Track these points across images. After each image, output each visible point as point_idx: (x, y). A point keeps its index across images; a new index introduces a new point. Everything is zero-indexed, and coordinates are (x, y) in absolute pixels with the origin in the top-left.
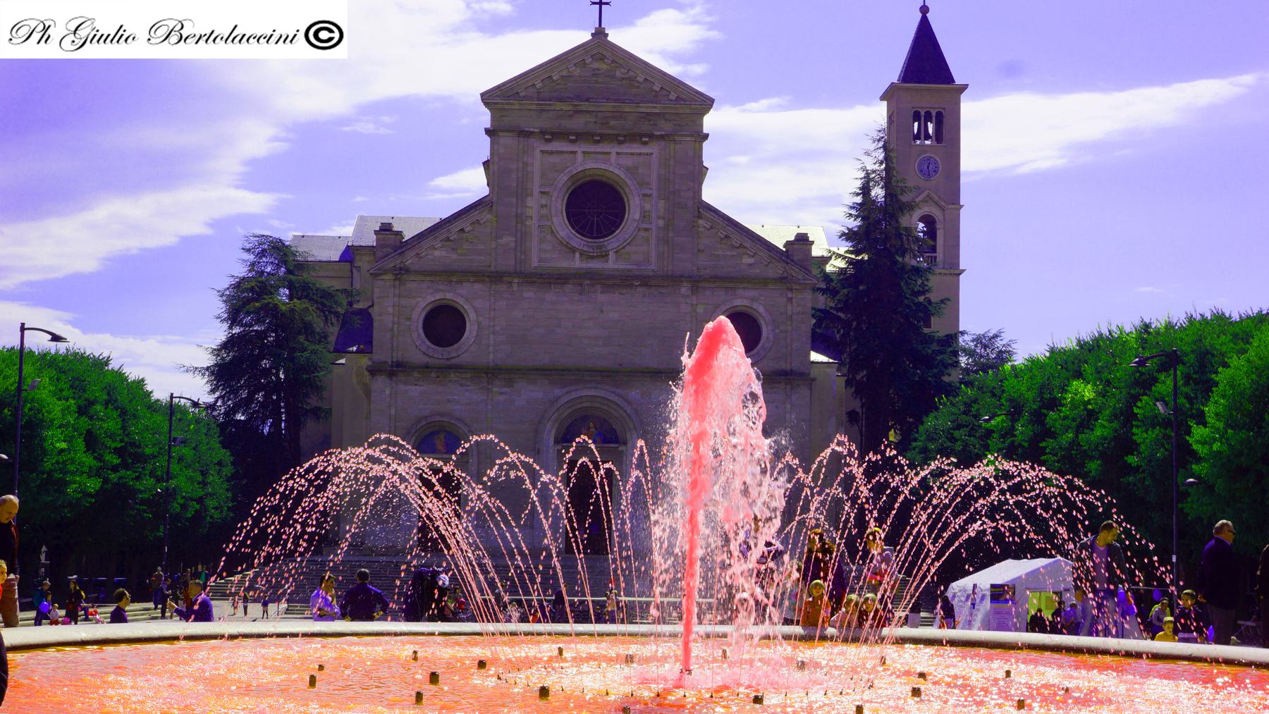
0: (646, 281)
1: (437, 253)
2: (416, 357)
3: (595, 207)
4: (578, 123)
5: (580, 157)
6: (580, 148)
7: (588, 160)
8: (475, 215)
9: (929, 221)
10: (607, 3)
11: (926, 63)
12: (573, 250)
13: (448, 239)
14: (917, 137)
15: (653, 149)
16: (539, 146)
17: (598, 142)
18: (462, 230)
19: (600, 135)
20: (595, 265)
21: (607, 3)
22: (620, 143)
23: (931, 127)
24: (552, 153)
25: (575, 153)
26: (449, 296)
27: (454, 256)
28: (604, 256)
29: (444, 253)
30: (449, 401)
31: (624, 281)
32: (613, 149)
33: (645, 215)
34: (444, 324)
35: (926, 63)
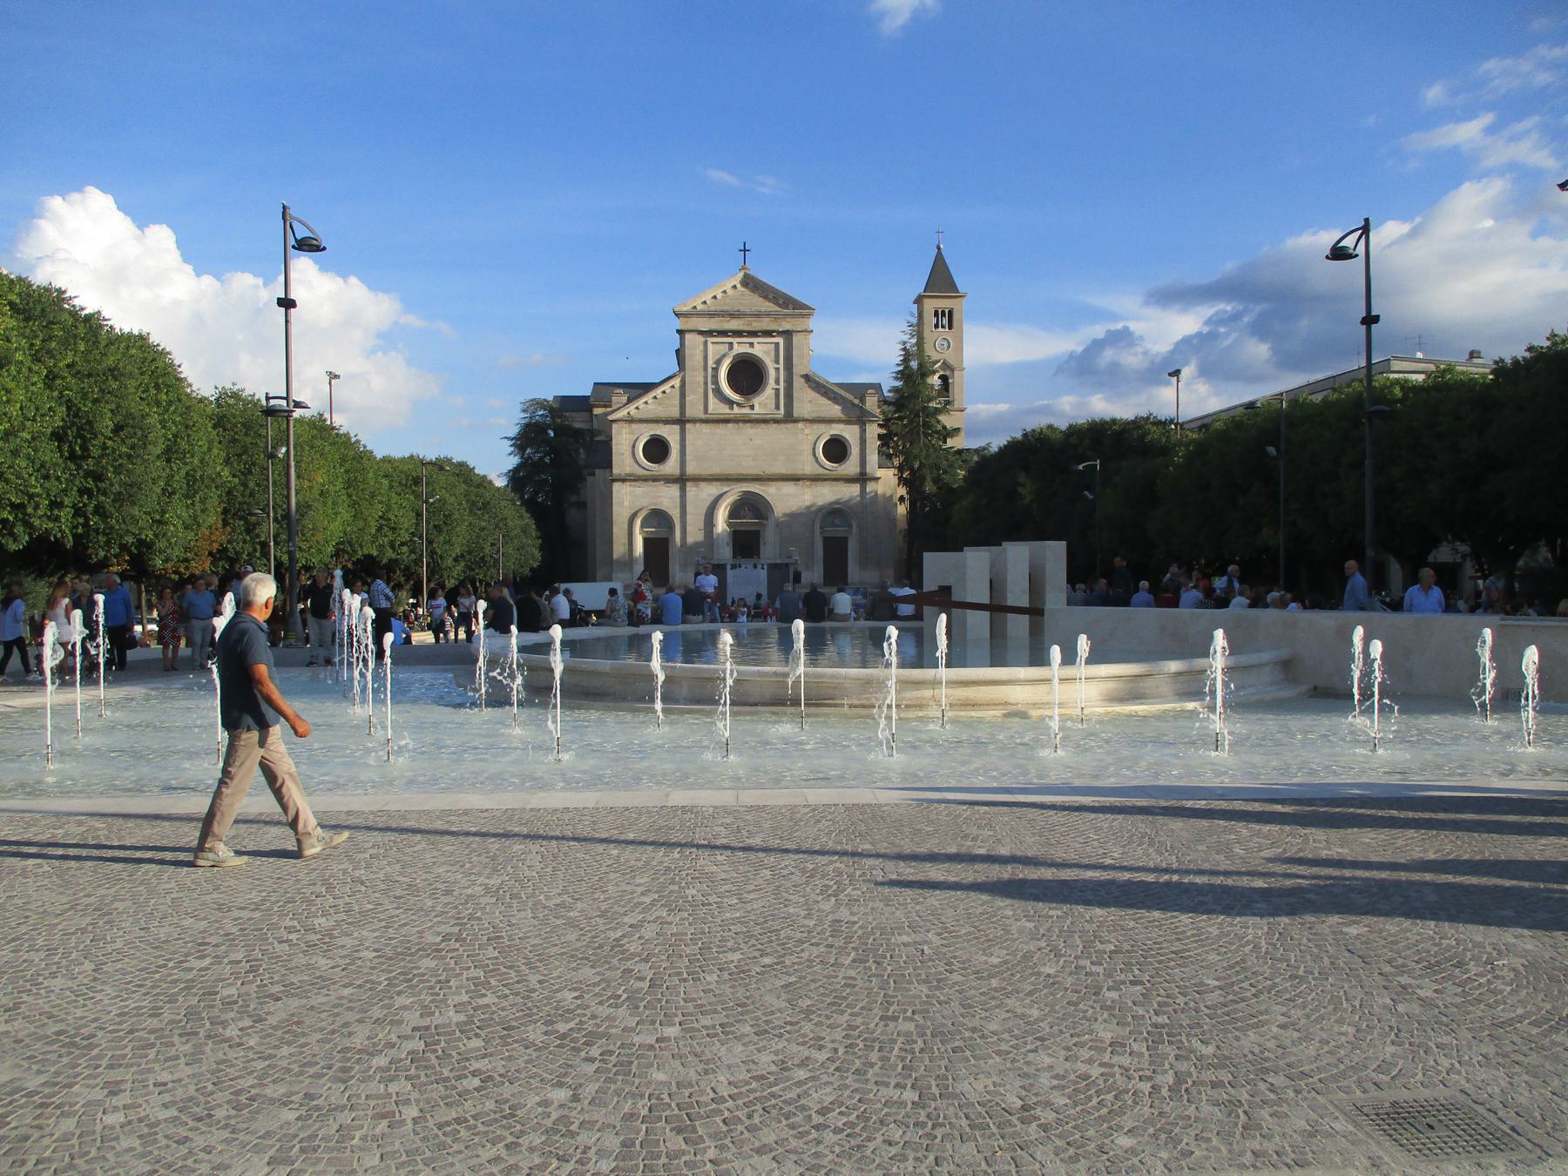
0: (776, 421)
3: (747, 375)
4: (734, 325)
5: (735, 346)
6: (735, 340)
7: (740, 347)
8: (672, 383)
9: (944, 378)
11: (940, 280)
12: (731, 403)
14: (936, 326)
15: (781, 340)
16: (710, 340)
20: (746, 411)
23: (945, 321)
28: (752, 407)
31: (764, 421)
32: (755, 340)
33: (777, 382)
34: (657, 450)
35: (940, 280)
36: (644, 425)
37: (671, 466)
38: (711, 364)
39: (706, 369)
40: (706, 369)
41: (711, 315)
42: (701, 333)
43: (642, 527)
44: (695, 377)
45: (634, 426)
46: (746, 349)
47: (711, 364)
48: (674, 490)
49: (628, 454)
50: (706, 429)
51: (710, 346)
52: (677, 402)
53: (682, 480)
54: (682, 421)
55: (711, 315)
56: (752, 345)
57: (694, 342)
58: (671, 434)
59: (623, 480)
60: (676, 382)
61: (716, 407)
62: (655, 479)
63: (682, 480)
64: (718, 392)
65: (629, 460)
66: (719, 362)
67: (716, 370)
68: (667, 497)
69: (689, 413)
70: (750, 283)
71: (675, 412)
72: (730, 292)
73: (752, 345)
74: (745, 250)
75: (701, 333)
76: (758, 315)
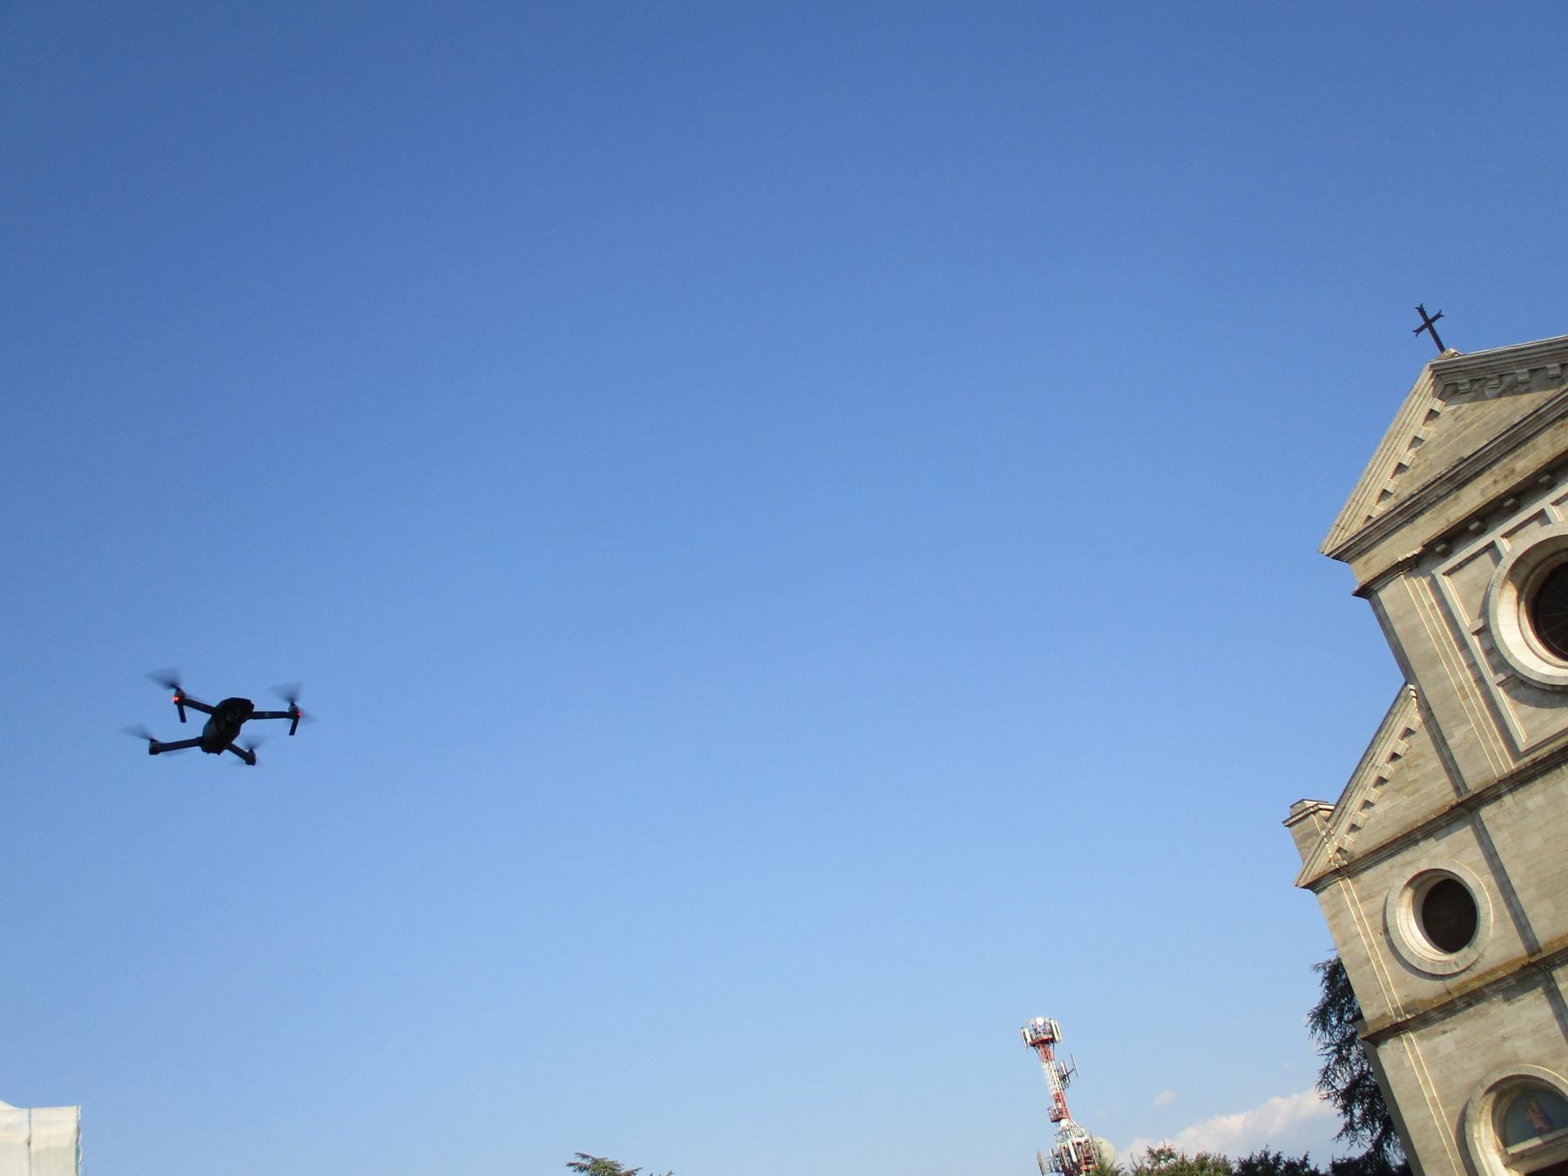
1: (1378, 809)
2: (1428, 990)
4: (1472, 498)
5: (1505, 546)
6: (1494, 535)
8: (1400, 726)
10: (1421, 310)
13: (1381, 781)
17: (1515, 509)
18: (1395, 756)
19: (1510, 493)
21: (1421, 310)
22: (1550, 486)
24: (1460, 566)
25: (1491, 546)
26: (1424, 866)
27: (1403, 800)
29: (1387, 804)
30: (1504, 1038)
32: (1544, 503)
34: (1446, 909)
36: (1384, 866)
37: (1495, 940)
38: (1467, 622)
39: (1463, 645)
40: (1463, 645)
41: (1409, 511)
42: (1411, 565)
43: (1506, 1141)
44: (1452, 676)
45: (1367, 877)
46: (1536, 535)
47: (1467, 622)
48: (1533, 1009)
49: (1380, 955)
50: (1535, 797)
51: (1447, 583)
52: (1434, 764)
53: (1534, 971)
54: (1466, 809)
55: (1409, 511)
56: (1541, 516)
57: (1406, 594)
58: (1453, 854)
59: (1397, 1030)
60: (1414, 717)
61: (1531, 726)
62: (1469, 998)
63: (1534, 971)
64: (1520, 684)
65: (1387, 971)
66: (1485, 612)
67: (1484, 632)
68: (1522, 1034)
69: (1474, 780)
70: (1457, 381)
71: (1441, 794)
72: (1429, 432)
73: (1541, 516)
74: (1429, 323)
75: (1411, 565)
76: (1515, 439)
